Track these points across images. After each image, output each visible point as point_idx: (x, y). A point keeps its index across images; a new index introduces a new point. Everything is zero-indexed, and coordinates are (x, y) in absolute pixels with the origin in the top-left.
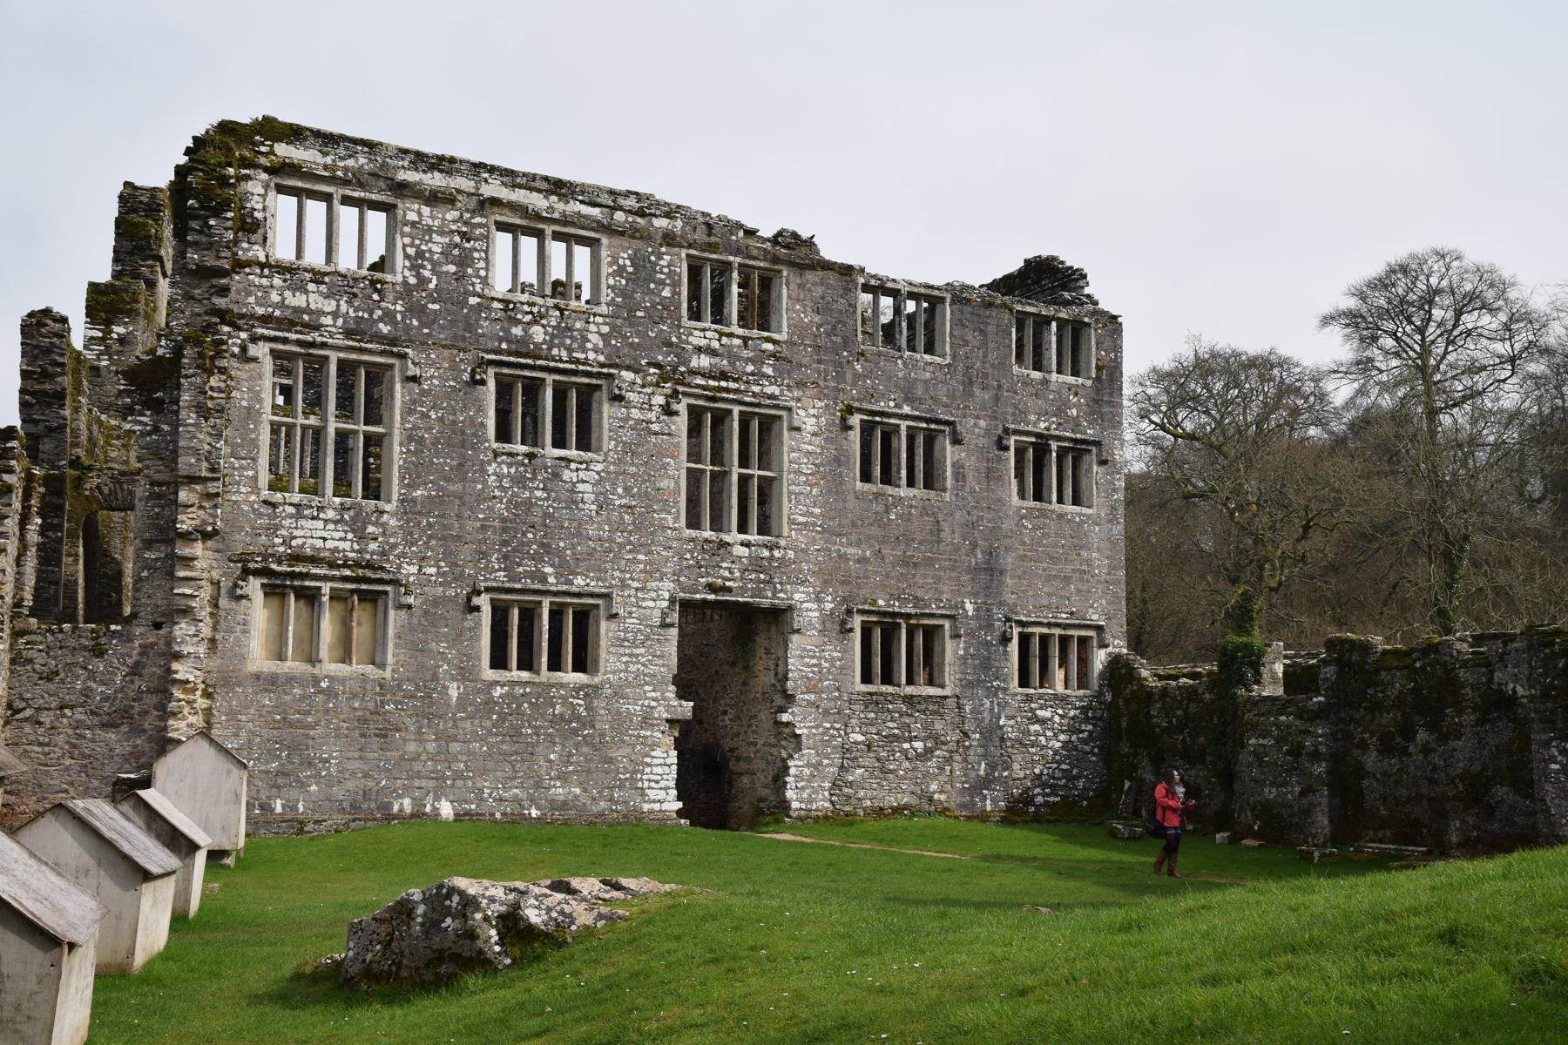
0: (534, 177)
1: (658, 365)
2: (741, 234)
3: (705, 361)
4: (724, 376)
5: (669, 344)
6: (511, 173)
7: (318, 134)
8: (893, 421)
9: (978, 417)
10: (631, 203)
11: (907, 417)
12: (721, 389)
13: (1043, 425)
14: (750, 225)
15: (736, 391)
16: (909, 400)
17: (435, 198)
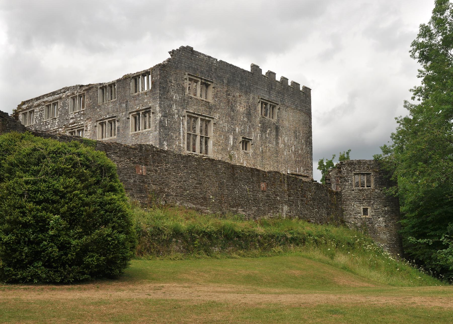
0: (50, 93)
1: (64, 125)
2: (79, 87)
3: (71, 121)
4: (75, 123)
5: (67, 120)
6: (47, 95)
7: (26, 101)
8: (105, 121)
9: (123, 112)
10: (63, 90)
11: (107, 119)
12: (73, 127)
13: (138, 108)
14: (81, 84)
15: (77, 126)
16: (108, 113)
17: (39, 105)
